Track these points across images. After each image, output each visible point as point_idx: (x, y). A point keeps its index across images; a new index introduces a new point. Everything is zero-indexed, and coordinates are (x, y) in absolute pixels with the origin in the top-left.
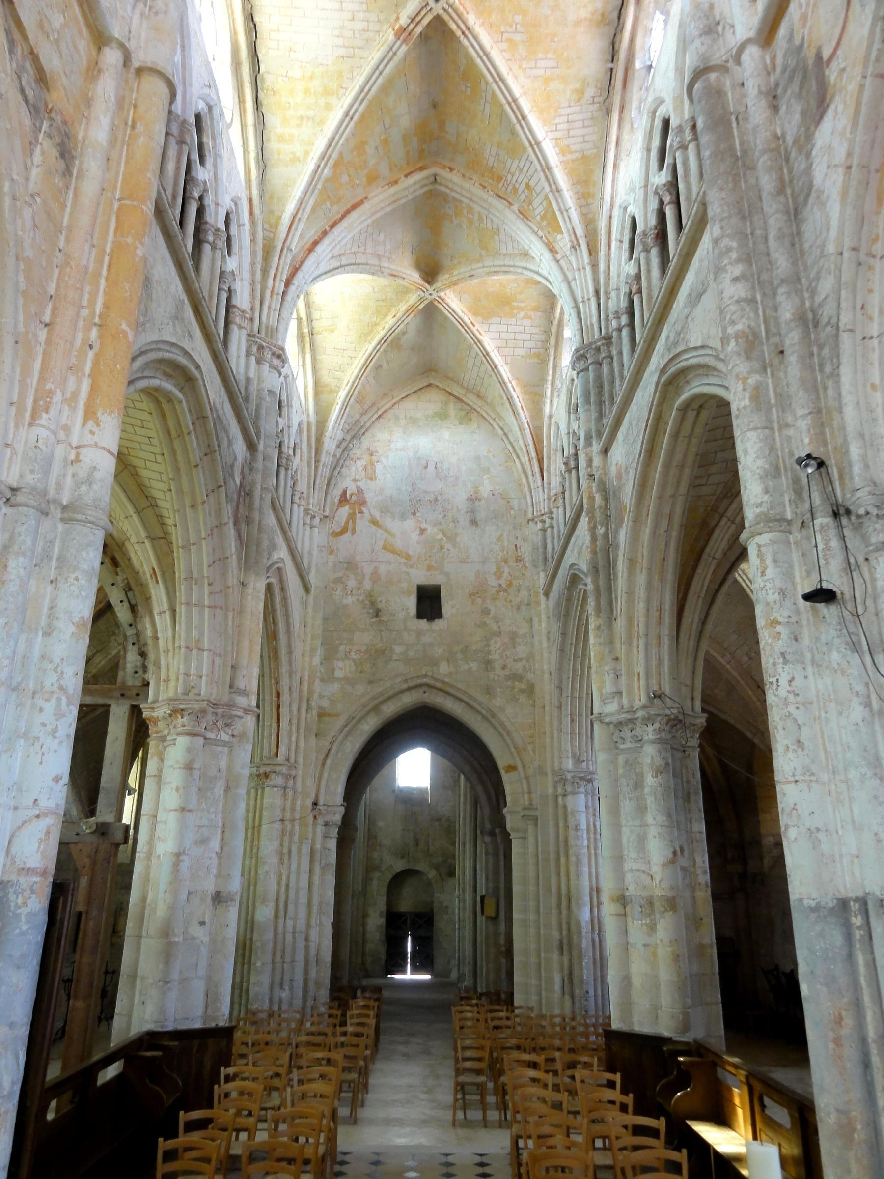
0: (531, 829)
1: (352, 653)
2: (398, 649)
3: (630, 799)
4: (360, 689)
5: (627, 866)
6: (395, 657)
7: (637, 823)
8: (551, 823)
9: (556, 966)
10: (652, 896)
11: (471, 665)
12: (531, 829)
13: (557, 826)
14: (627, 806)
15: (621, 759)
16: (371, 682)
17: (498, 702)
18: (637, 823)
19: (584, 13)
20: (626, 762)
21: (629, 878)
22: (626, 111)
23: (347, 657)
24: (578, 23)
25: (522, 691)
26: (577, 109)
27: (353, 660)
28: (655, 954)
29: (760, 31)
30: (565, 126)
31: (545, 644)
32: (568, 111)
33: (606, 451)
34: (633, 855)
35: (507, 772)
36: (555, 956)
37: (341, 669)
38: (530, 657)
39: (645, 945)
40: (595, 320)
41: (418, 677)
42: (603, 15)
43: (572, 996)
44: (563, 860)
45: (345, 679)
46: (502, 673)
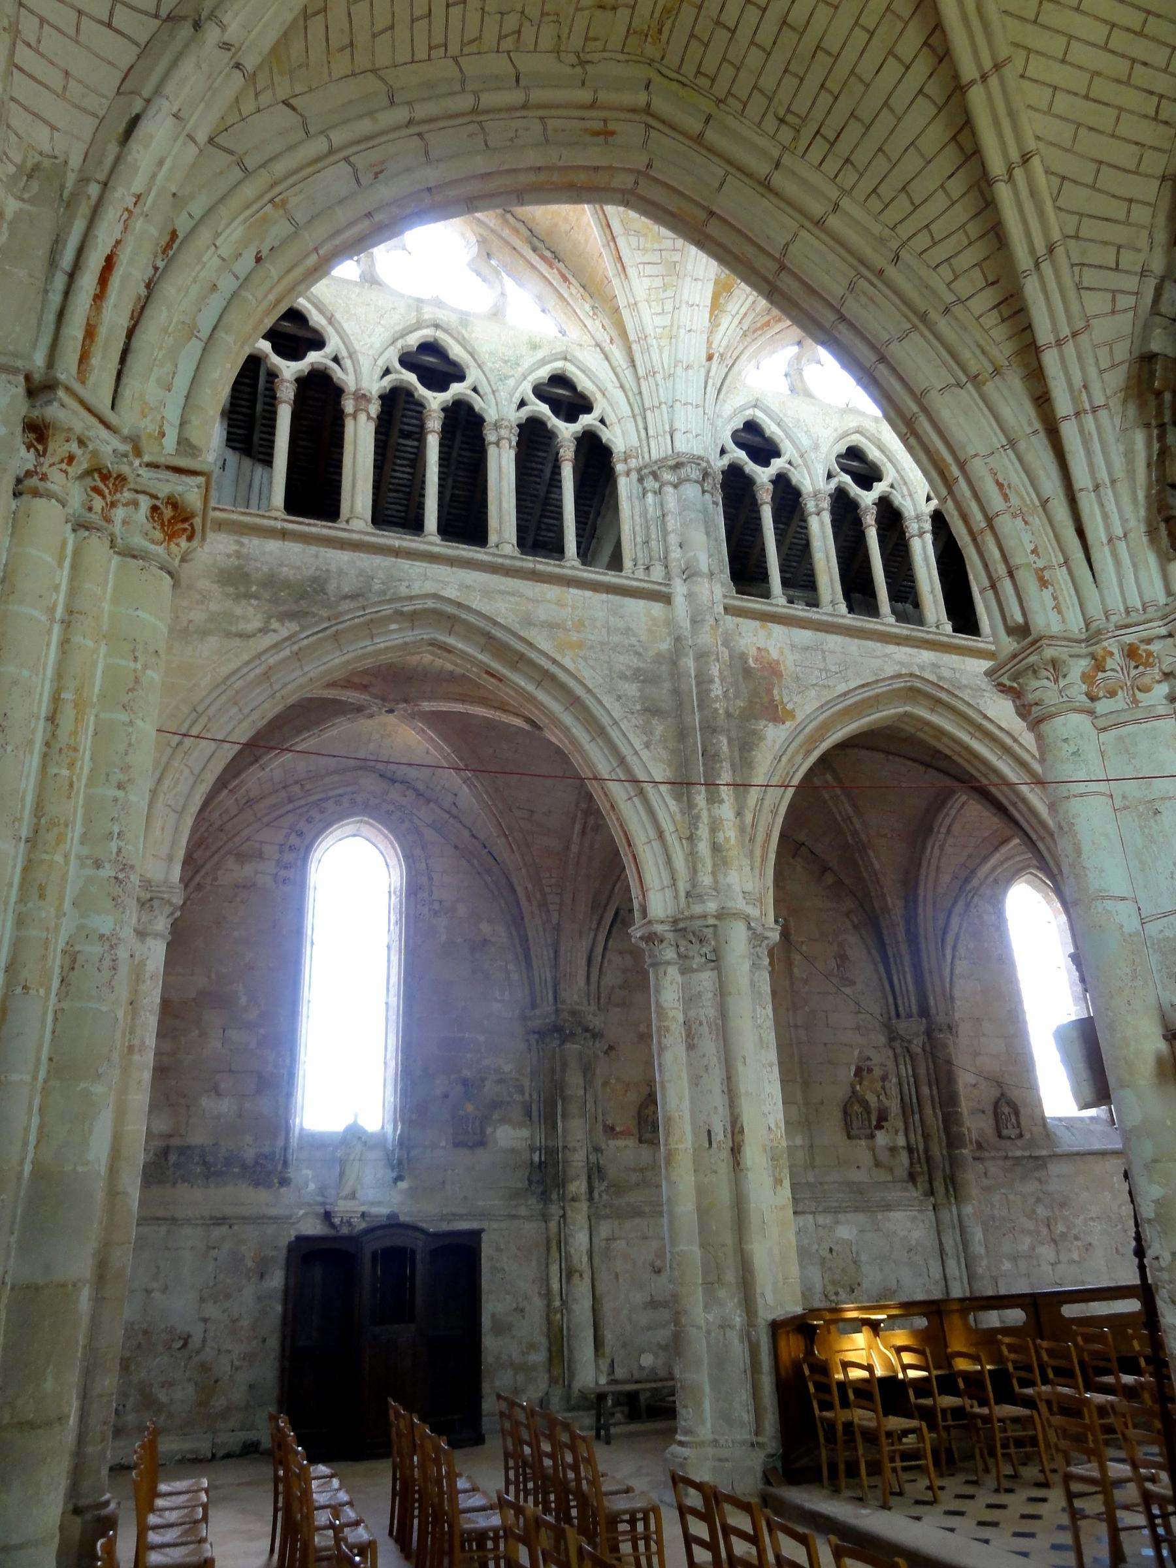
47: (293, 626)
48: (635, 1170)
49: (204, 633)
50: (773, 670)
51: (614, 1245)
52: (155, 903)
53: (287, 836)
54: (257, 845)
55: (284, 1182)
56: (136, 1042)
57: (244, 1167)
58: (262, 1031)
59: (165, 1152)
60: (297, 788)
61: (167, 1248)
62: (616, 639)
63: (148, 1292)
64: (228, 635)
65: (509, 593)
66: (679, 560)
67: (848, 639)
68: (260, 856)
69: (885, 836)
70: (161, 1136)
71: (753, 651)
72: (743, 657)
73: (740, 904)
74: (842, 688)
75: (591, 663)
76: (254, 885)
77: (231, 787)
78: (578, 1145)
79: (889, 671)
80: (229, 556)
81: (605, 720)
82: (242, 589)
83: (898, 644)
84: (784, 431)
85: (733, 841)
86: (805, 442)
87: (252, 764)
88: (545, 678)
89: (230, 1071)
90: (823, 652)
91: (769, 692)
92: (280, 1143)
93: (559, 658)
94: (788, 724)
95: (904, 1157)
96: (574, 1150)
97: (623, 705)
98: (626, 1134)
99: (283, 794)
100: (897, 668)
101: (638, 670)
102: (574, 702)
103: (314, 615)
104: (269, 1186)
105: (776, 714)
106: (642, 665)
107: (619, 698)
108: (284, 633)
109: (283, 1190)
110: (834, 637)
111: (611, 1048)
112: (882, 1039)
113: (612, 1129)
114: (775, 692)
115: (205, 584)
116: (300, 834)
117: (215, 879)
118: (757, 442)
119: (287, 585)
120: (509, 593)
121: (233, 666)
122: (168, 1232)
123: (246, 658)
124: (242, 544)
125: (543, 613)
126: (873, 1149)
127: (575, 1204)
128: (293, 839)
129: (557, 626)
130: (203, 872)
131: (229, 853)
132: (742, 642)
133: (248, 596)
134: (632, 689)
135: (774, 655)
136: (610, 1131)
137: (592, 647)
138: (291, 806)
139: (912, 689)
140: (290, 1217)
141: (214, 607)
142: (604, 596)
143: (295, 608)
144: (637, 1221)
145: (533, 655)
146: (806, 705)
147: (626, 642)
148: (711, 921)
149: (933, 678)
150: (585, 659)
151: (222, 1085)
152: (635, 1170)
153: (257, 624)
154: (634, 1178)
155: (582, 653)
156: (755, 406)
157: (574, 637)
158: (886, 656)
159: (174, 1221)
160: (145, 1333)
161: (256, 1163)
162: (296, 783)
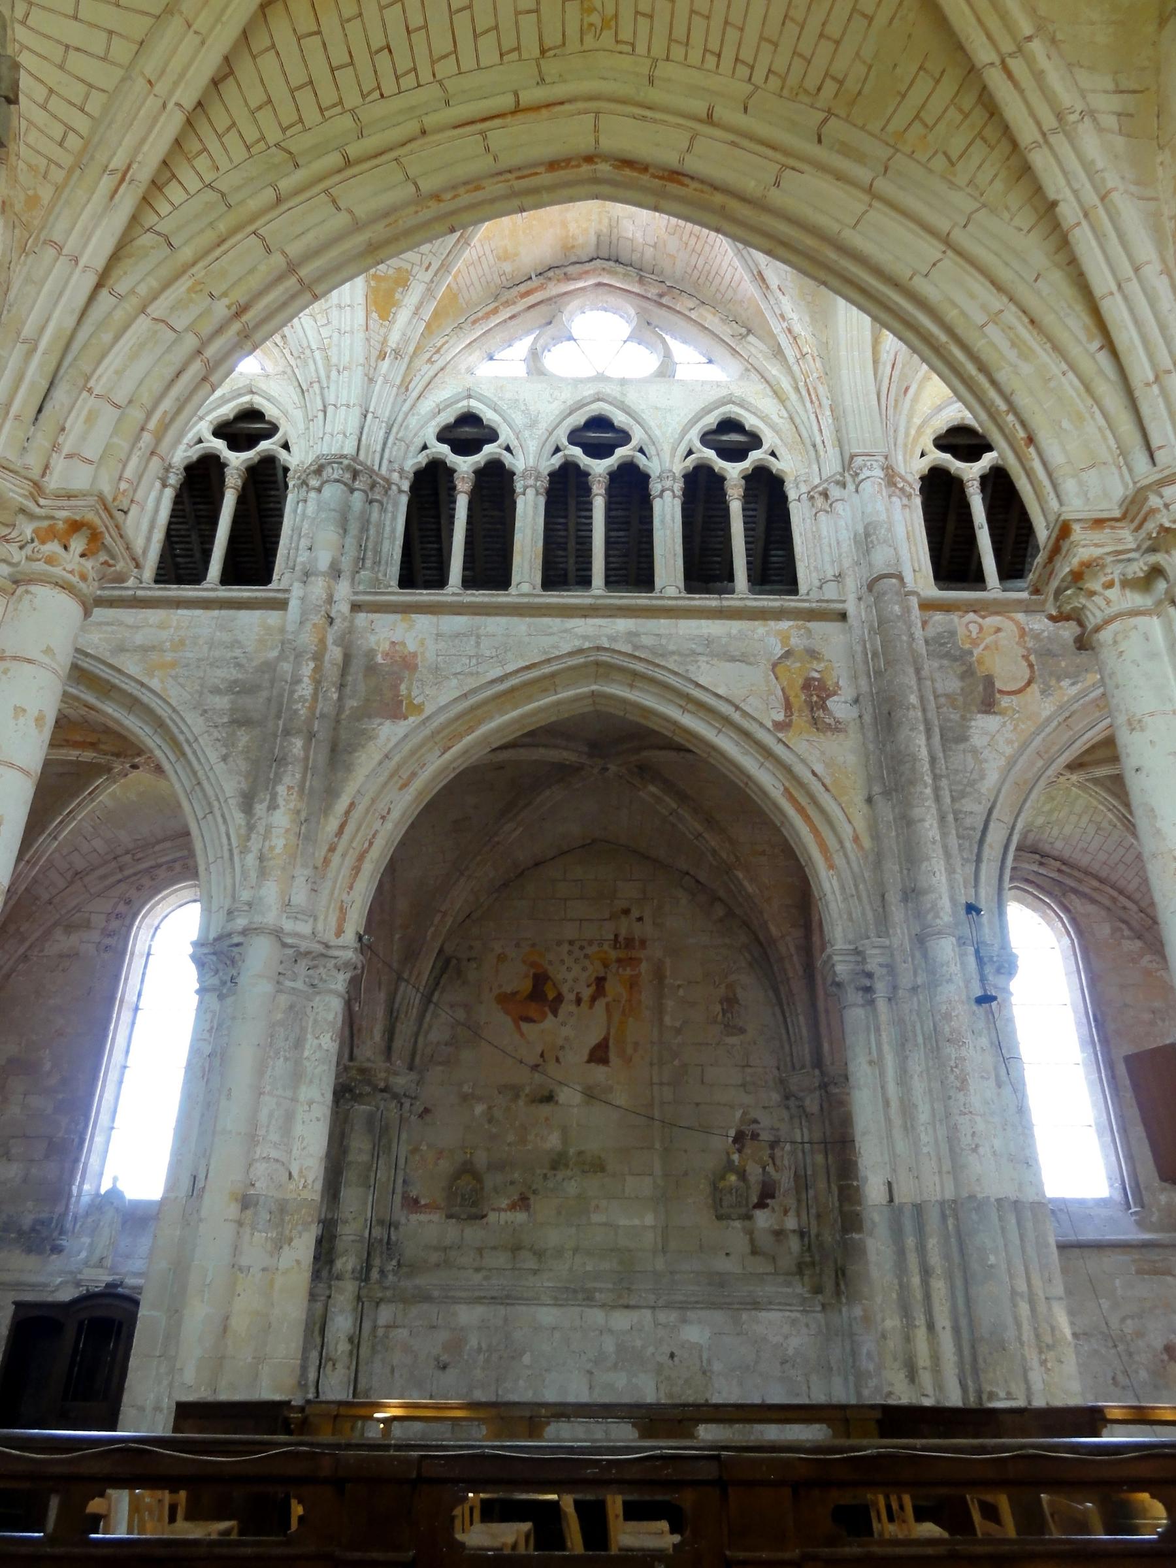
3: (286, 1059)
5: (259, 1152)
7: (289, 1094)
10: (286, 1201)
14: (280, 1067)
15: (283, 1000)
18: (289, 1094)
19: (573, 228)
20: (291, 1007)
21: (260, 1168)
22: (513, 322)
24: (564, 224)
26: (492, 261)
28: (272, 1282)
29: (925, 599)
30: (475, 257)
32: (488, 252)
33: (356, 607)
34: (274, 1137)
39: (264, 1270)
40: (379, 448)
42: (573, 247)
48: (436, 1249)
50: (407, 664)
51: (394, 1333)
53: (117, 904)
54: (87, 915)
55: (57, 1250)
57: (21, 1233)
58: (60, 1096)
60: (128, 858)
62: (217, 653)
65: (108, 624)
66: (303, 563)
67: (516, 620)
68: (87, 925)
69: (763, 853)
71: (386, 646)
72: (370, 654)
73: (271, 916)
74: (497, 672)
75: (181, 680)
76: (77, 954)
78: (350, 1217)
79: (566, 648)
81: (181, 738)
83: (585, 616)
84: (500, 415)
85: (278, 850)
86: (519, 419)
88: (133, 704)
89: (25, 1136)
90: (478, 637)
91: (395, 687)
92: (60, 1209)
93: (145, 680)
94: (411, 719)
95: (794, 1243)
96: (346, 1222)
97: (207, 720)
98: (432, 1207)
99: (113, 864)
100: (577, 643)
101: (236, 682)
102: (159, 724)
104: (40, 1252)
105: (396, 709)
106: (240, 676)
107: (205, 711)
109: (54, 1257)
110: (498, 619)
111: (427, 1110)
112: (775, 1097)
113: (416, 1201)
114: (403, 687)
116: (128, 902)
117: (42, 951)
118: (468, 432)
120: (108, 624)
125: (139, 639)
126: (750, 1233)
127: (340, 1283)
128: (121, 908)
129: (153, 648)
130: (27, 944)
131: (55, 924)
132: (373, 639)
134: (222, 702)
135: (412, 647)
136: (413, 1204)
137: (187, 665)
138: (120, 876)
139: (598, 664)
140: (46, 1285)
142: (216, 613)
144: (425, 1306)
145: (116, 680)
146: (437, 697)
147: (229, 655)
148: (236, 940)
149: (627, 648)
150: (175, 678)
151: (13, 1151)
152: (436, 1249)
154: (434, 1257)
155: (173, 673)
156: (469, 397)
157: (169, 657)
158: (566, 631)
161: (33, 1230)
162: (127, 853)
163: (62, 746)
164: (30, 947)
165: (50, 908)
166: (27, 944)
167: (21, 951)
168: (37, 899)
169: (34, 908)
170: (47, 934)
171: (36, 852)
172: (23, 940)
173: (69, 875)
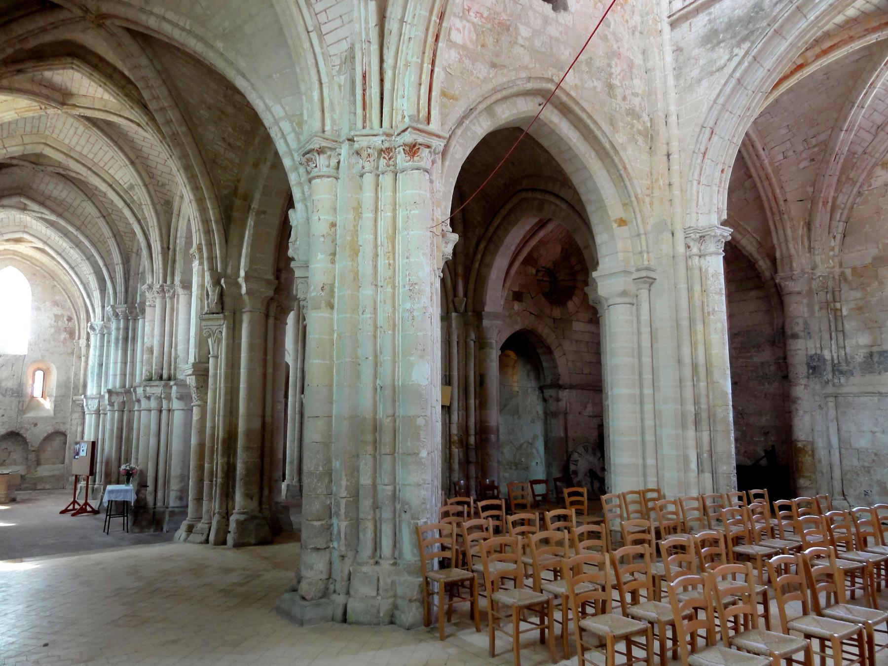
0: (644, 294)
1: (472, 14)
2: (524, 32)
4: (482, 70)
6: (520, 41)
8: (683, 286)
9: (691, 443)
11: (596, 83)
12: (644, 294)
13: (690, 290)
16: (494, 65)
17: (620, 139)
23: (464, 14)
25: (639, 132)
27: (474, 24)
31: (671, 81)
35: (620, 226)
36: (691, 433)
37: (458, 30)
38: (650, 94)
41: (542, 79)
43: (714, 473)
44: (699, 327)
45: (463, 47)
46: (625, 105)
47: (746, 45)
49: (699, 81)
52: (707, 238)
56: (710, 310)
59: (871, 354)
61: (879, 409)
63: (873, 433)
64: (712, 73)
70: (866, 346)
77: (845, 128)
80: (705, 26)
82: (715, 41)
87: (851, 109)
103: (758, 29)
108: (741, 52)
115: (696, 52)
119: (740, 20)
121: (717, 91)
122: (879, 400)
123: (723, 82)
124: (710, 14)
130: (858, 184)
131: (875, 165)
133: (718, 44)
141: (702, 62)
143: (746, 32)
153: (727, 57)
159: (880, 394)
160: (876, 454)
163: (865, 35)
164: (861, 187)
165: (866, 156)
166: (858, 184)
167: (855, 190)
168: (855, 153)
169: (855, 160)
170: (870, 174)
171: (851, 122)
172: (854, 183)
173: (873, 130)
